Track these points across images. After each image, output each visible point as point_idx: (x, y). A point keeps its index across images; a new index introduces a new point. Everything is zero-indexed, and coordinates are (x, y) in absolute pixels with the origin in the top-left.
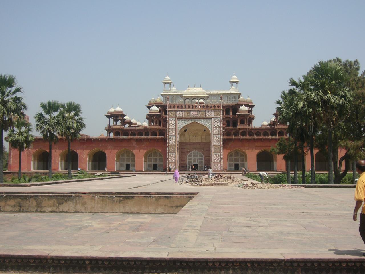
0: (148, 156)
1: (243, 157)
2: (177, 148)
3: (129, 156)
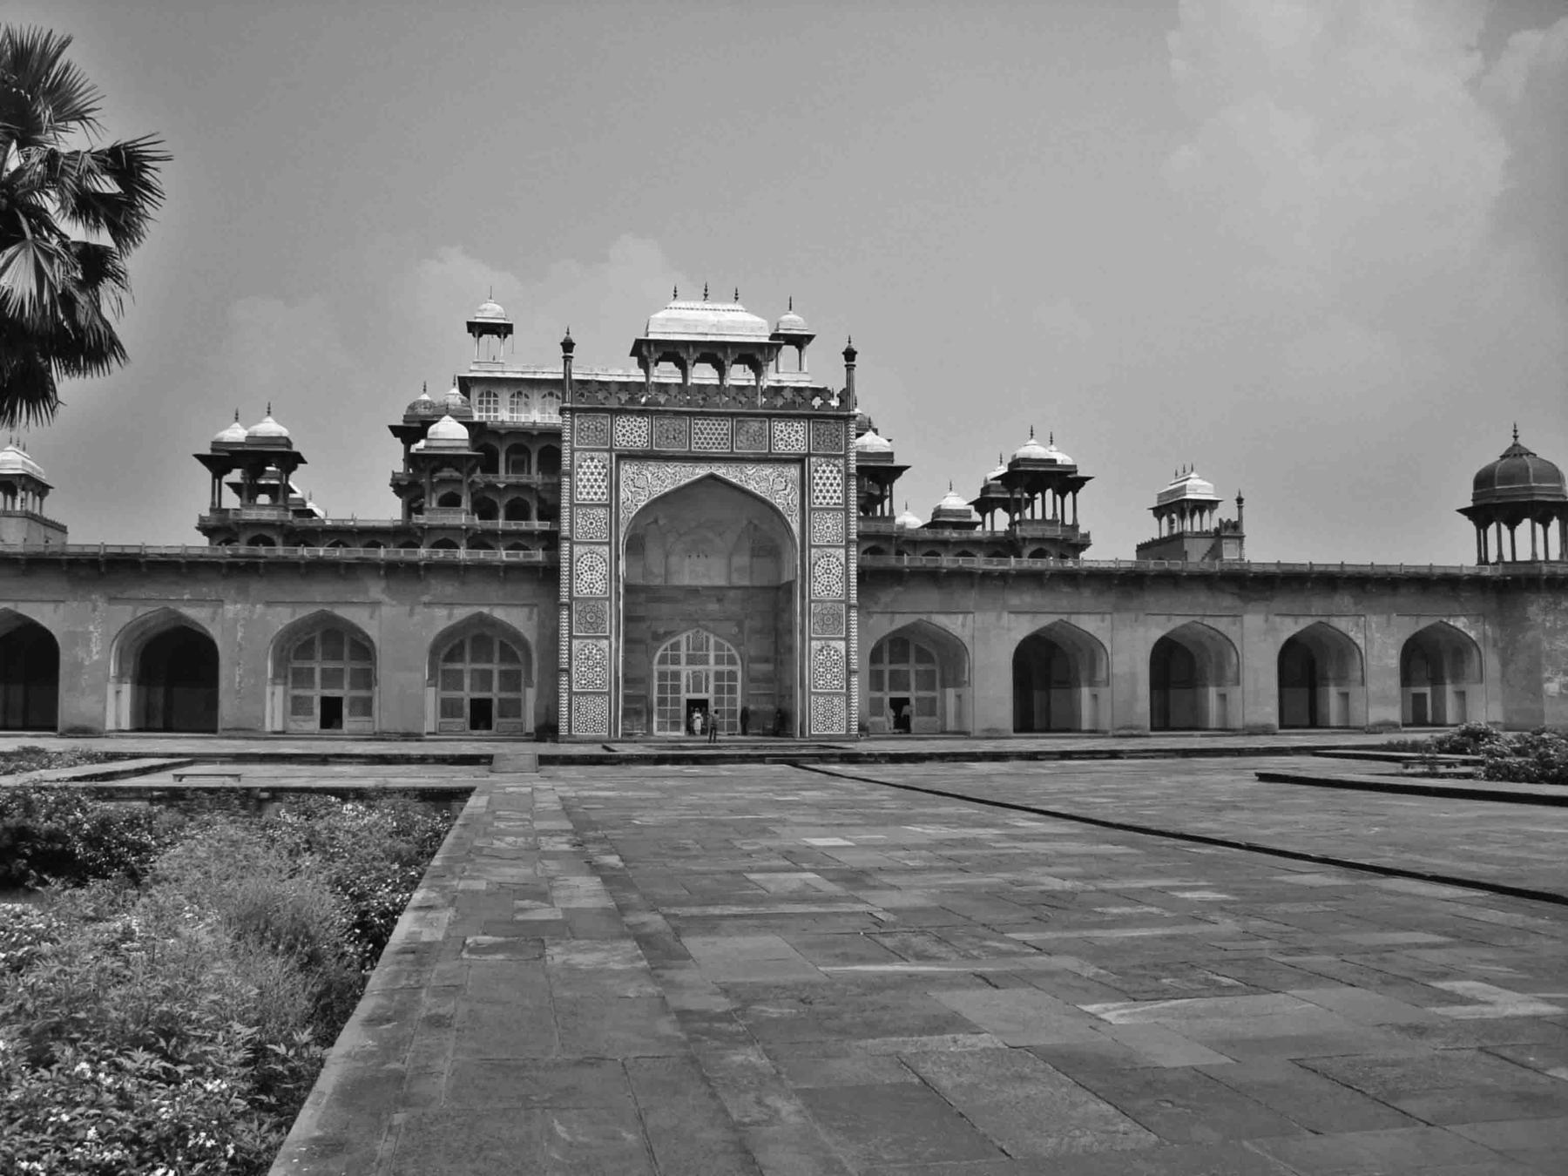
1: (929, 667)
3: (337, 656)
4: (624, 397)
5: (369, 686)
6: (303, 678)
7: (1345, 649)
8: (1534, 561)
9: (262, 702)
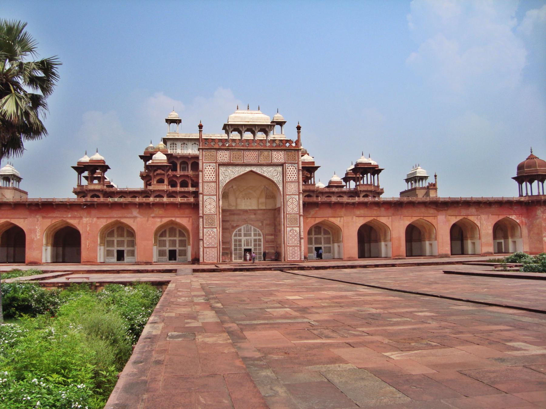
0: (159, 235)
1: (328, 236)
2: (217, 220)
3: (122, 236)
4: (220, 144)
5: (133, 246)
6: (110, 243)
7: (473, 227)
8: (539, 195)
9: (96, 251)
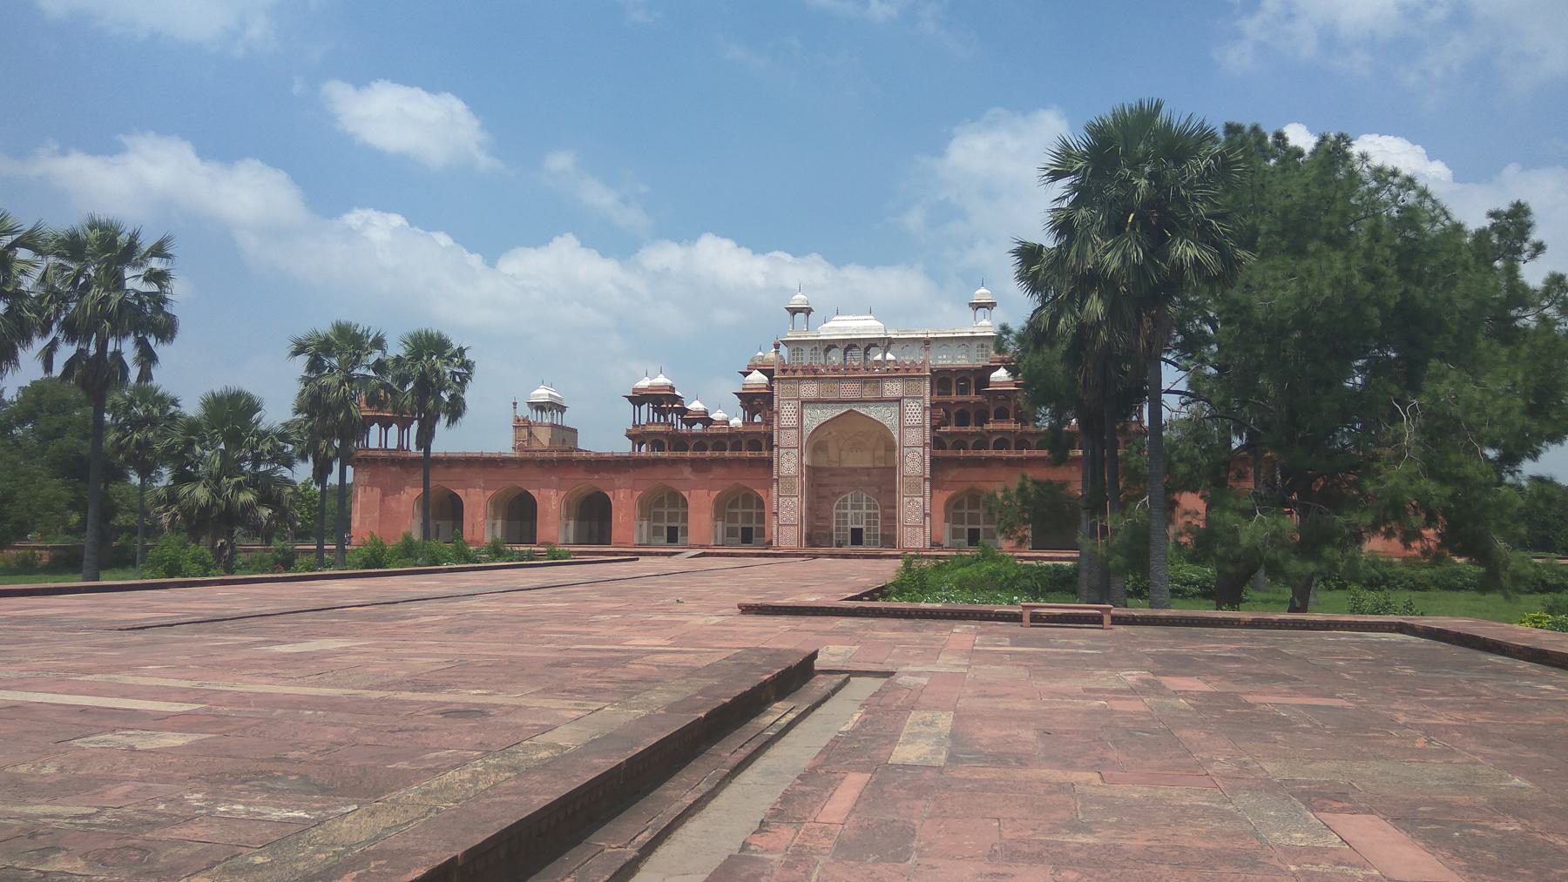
2: (799, 484)
